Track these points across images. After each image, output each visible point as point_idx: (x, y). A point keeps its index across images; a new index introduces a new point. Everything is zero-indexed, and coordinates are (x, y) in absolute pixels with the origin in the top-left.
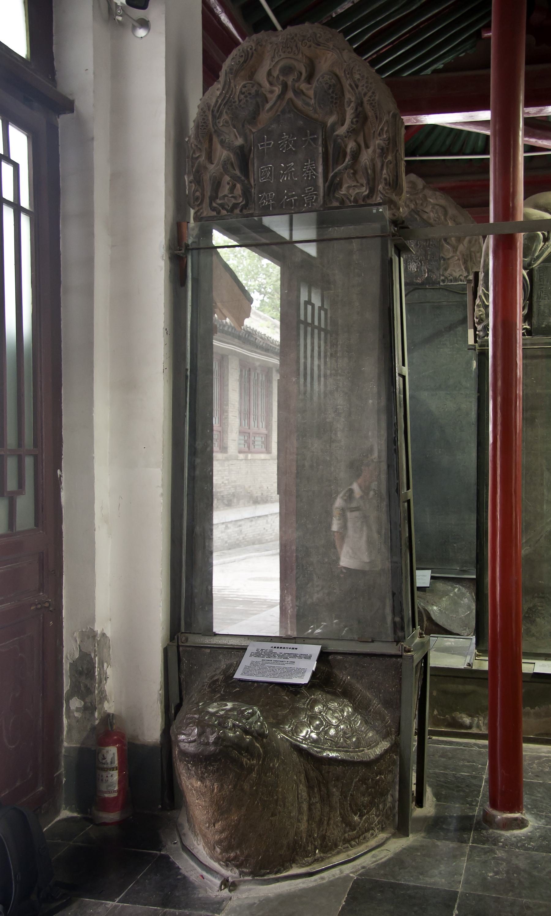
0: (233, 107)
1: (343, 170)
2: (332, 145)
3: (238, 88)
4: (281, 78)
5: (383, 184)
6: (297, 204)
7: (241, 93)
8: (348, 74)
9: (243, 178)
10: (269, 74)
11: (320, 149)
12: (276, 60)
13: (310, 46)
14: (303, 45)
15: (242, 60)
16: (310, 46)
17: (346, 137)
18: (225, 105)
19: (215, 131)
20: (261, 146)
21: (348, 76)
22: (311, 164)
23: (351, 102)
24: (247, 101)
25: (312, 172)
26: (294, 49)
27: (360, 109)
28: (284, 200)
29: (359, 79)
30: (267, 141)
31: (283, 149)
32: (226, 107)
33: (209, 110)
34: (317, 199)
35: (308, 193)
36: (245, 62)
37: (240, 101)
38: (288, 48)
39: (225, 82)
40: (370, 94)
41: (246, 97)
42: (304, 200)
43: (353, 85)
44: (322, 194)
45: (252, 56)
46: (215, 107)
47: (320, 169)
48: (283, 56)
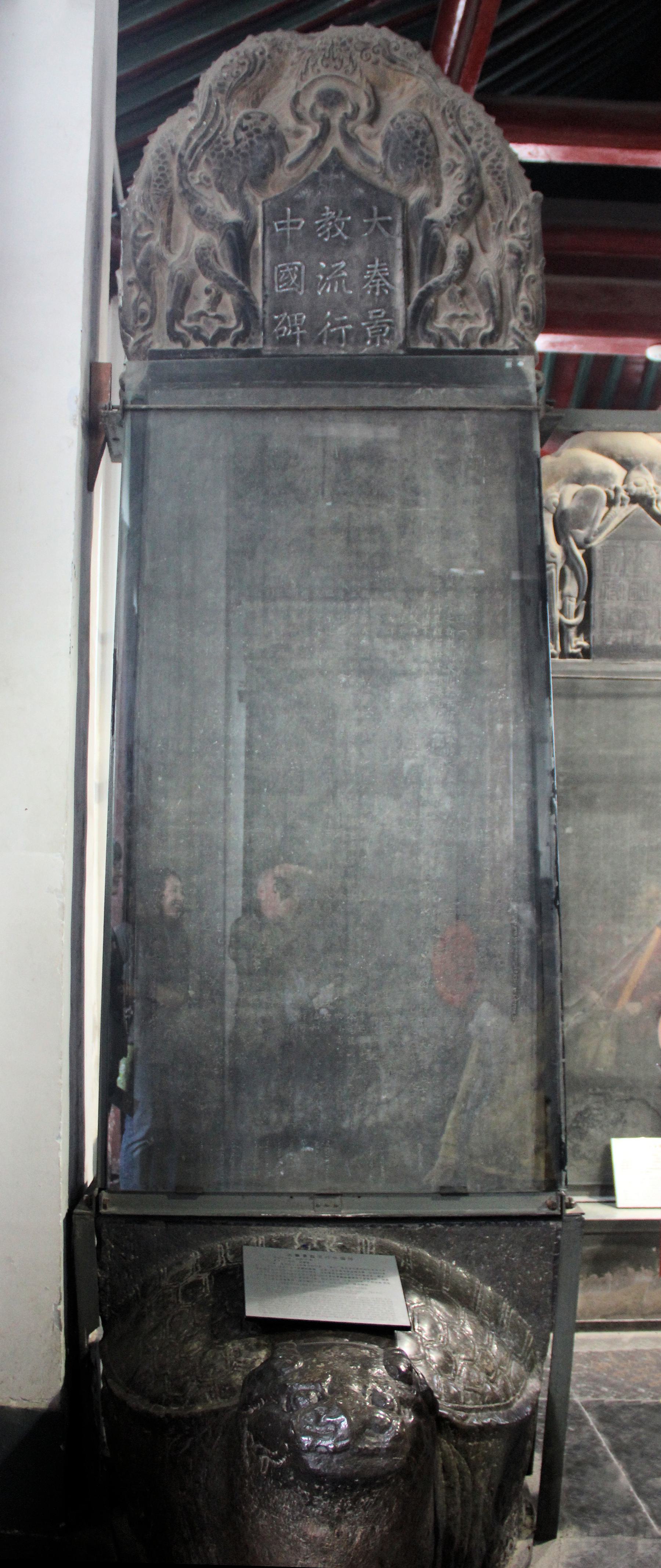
0: (223, 151)
1: (444, 283)
2: (420, 239)
3: (234, 123)
4: (320, 111)
5: (521, 317)
6: (352, 339)
7: (240, 127)
8: (451, 117)
9: (240, 282)
10: (296, 100)
11: (399, 242)
12: (311, 77)
13: (376, 63)
14: (364, 58)
15: (244, 71)
16: (376, 63)
17: (448, 226)
18: (205, 147)
19: (185, 193)
20: (280, 226)
21: (450, 121)
22: (379, 268)
23: (456, 166)
24: (252, 143)
25: (381, 282)
26: (346, 62)
27: (474, 180)
28: (325, 328)
29: (471, 129)
30: (292, 217)
31: (325, 236)
32: (208, 150)
33: (173, 152)
34: (391, 332)
35: (374, 320)
36: (249, 74)
37: (237, 142)
38: (334, 59)
39: (208, 106)
40: (492, 155)
41: (250, 135)
42: (366, 331)
43: (461, 138)
44: (401, 324)
45: (262, 67)
46: (186, 149)
47: (399, 278)
48: (324, 72)
